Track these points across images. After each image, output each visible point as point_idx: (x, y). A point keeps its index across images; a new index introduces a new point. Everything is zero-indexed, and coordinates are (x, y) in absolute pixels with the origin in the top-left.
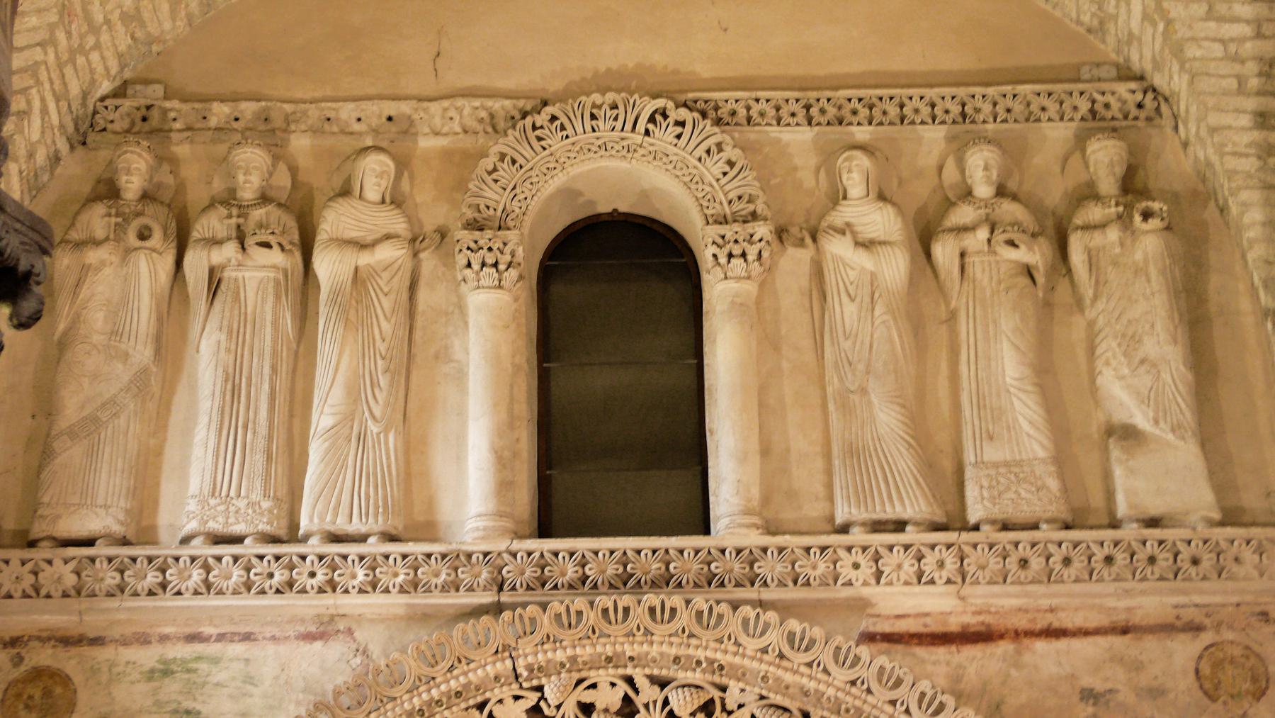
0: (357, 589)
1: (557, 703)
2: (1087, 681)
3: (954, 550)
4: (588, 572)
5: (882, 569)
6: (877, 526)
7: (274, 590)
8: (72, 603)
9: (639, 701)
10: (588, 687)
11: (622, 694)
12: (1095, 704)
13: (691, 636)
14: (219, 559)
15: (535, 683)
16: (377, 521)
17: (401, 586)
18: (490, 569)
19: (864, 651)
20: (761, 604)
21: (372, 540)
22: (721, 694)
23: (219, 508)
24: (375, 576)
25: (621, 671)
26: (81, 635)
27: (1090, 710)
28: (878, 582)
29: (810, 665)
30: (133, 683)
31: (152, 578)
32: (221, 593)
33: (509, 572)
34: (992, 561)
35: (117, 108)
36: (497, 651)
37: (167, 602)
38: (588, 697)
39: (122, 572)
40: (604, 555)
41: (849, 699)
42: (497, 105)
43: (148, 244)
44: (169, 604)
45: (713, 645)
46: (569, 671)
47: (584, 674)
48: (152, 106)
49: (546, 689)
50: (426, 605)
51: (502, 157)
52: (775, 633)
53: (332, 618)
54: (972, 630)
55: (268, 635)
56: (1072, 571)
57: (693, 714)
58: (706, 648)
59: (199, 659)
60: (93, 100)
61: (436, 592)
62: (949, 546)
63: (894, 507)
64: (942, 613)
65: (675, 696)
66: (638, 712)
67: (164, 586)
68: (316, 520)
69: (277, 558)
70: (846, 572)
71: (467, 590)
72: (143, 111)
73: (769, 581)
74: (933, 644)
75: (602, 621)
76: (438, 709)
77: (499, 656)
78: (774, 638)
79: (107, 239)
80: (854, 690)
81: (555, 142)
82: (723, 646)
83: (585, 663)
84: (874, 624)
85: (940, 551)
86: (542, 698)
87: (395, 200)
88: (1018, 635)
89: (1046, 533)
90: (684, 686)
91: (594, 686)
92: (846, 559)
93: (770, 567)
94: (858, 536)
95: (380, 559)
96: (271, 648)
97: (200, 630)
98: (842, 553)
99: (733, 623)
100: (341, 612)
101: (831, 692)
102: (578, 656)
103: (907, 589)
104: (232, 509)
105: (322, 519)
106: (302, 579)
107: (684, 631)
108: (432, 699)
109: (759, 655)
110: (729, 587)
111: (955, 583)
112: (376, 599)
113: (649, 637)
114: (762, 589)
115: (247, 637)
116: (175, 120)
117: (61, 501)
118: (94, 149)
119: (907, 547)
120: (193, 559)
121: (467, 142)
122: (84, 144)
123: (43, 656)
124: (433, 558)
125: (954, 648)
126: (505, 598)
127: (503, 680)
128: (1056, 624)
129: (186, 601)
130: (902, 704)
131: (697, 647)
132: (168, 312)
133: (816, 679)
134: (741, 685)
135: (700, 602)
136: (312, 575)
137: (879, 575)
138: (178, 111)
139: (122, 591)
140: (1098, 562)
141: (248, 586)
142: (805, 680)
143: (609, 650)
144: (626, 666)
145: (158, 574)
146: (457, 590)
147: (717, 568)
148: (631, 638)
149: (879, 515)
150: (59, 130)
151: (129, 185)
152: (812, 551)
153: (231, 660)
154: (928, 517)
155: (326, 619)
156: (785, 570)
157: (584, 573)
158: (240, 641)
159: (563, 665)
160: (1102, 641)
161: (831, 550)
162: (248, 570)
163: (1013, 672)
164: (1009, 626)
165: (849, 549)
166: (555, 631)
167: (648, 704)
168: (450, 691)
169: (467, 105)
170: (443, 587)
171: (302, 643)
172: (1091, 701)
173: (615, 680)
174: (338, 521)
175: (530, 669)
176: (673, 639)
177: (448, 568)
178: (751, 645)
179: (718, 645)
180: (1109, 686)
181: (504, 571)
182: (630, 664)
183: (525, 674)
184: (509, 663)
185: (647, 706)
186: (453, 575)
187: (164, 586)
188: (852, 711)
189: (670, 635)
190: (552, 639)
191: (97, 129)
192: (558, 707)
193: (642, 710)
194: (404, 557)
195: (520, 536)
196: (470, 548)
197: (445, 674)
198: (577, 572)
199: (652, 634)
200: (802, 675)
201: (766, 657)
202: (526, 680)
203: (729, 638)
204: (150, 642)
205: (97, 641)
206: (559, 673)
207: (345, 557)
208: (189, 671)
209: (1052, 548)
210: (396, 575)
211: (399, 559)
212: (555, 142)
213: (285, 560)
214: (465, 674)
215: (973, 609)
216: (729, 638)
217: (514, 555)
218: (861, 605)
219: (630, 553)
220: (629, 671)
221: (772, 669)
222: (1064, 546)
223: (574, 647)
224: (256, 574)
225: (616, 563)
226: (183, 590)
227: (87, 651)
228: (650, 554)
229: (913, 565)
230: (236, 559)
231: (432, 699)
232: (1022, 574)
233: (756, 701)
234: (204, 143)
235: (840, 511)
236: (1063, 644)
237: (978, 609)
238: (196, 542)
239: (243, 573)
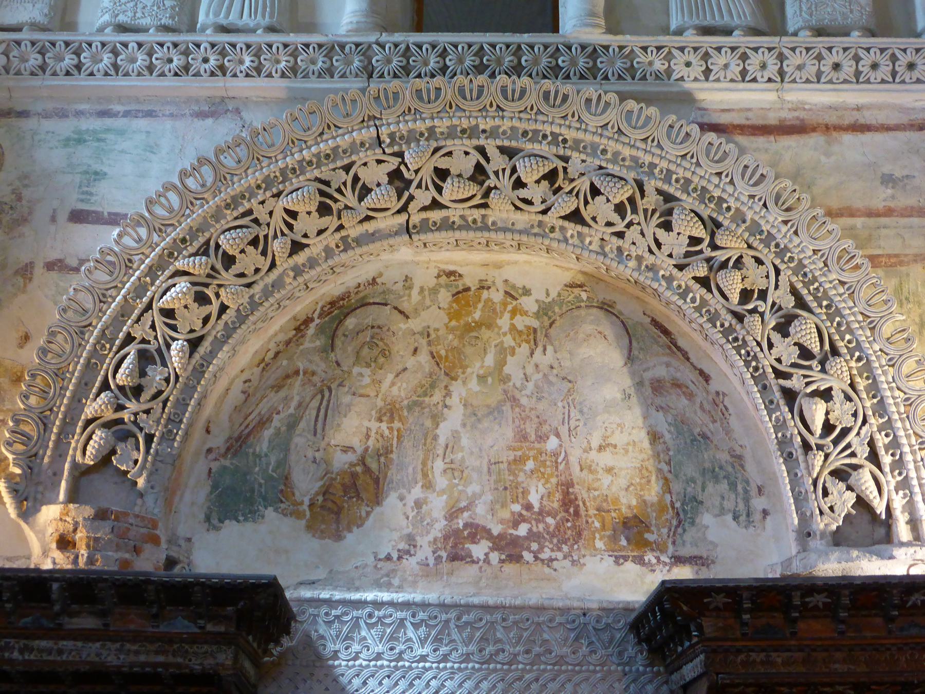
0: (244, 74)
1: (416, 168)
2: (887, 169)
3: (775, 53)
4: (448, 63)
5: (711, 67)
6: (707, 31)
7: (172, 72)
9: (490, 168)
10: (444, 155)
11: (474, 163)
12: (893, 188)
13: (539, 112)
14: (125, 45)
15: (396, 148)
16: (264, 16)
17: (283, 72)
18: (362, 58)
21: (259, 32)
22: (565, 165)
23: (128, 5)
24: (260, 63)
25: (475, 142)
26: (10, 109)
27: (890, 191)
28: (707, 79)
29: (645, 140)
30: (52, 148)
31: (69, 60)
32: (127, 74)
33: (377, 61)
34: (808, 62)
36: (363, 121)
37: (81, 81)
38: (443, 164)
39: (43, 55)
40: (463, 48)
41: (680, 171)
44: (83, 83)
45: (558, 121)
46: (427, 139)
47: (442, 143)
49: (406, 154)
50: (305, 89)
52: (615, 111)
53: (223, 99)
54: (788, 123)
55: (168, 113)
57: (538, 182)
58: (552, 123)
59: (108, 130)
61: (313, 78)
62: (770, 49)
63: (722, 16)
64: (762, 109)
65: (522, 164)
66: (489, 178)
67: (79, 67)
68: (211, 15)
69: (175, 45)
70: (679, 70)
71: (341, 77)
73: (610, 75)
74: (754, 135)
75: (459, 97)
76: (309, 168)
77: (365, 124)
80: (684, 163)
82: (567, 123)
83: (442, 133)
84: (702, 117)
85: (763, 53)
86: (403, 162)
88: (828, 128)
89: (855, 39)
90: (529, 156)
91: (449, 154)
92: (680, 59)
94: (691, 38)
95: (264, 47)
96: (168, 124)
97: (110, 107)
98: (676, 52)
100: (231, 94)
101: (664, 164)
102: (434, 127)
103: (733, 85)
104: (140, 6)
105: (217, 14)
106: (196, 65)
107: (532, 109)
108: (304, 159)
109: (599, 131)
110: (574, 79)
111: (775, 82)
112: (260, 82)
113: (501, 113)
114: (603, 82)
115: (150, 114)
119: (733, 49)
120: (103, 45)
124: (311, 48)
125: (772, 138)
127: (367, 145)
128: (862, 121)
130: (727, 176)
131: (544, 122)
133: (650, 152)
134: (583, 157)
136: (206, 60)
137: (707, 72)
139: (44, 71)
140: (901, 68)
141: (150, 68)
142: (640, 154)
143: (465, 124)
144: (478, 138)
145: (74, 56)
146: (332, 77)
147: (563, 61)
148: (484, 114)
149: (708, 21)
152: (649, 51)
153: (134, 132)
154: (752, 24)
155: (217, 100)
156: (625, 66)
157: (445, 64)
158: (143, 117)
159: (422, 134)
160: (900, 135)
161: (667, 50)
162: (150, 55)
163: (823, 158)
164: (820, 121)
165: (682, 49)
166: (416, 104)
167: (498, 171)
168: (319, 153)
170: (320, 73)
171: (196, 120)
172: (890, 185)
173: (468, 150)
174: (230, 18)
175: (392, 136)
176: (522, 115)
177: (325, 56)
178: (594, 122)
179: (562, 122)
180: (905, 173)
181: (374, 61)
182: (483, 136)
183: (388, 141)
184: (373, 130)
185: (496, 173)
186: (328, 63)
187: (79, 67)
188: (682, 181)
189: (521, 112)
190: (413, 111)
192: (417, 172)
193: (492, 176)
194: (286, 46)
195: (387, 27)
196: (344, 40)
197: (316, 138)
198: (438, 62)
199: (503, 110)
200: (638, 149)
201: (606, 133)
202: (388, 146)
203: (573, 116)
204: (67, 116)
205: (23, 114)
206: (418, 141)
207: (234, 46)
208: (99, 140)
209: (862, 53)
210: (278, 62)
211: (281, 47)
213: (182, 47)
214: (334, 138)
215: (790, 106)
216: (573, 116)
217: (383, 48)
219: (486, 47)
220: (482, 142)
221: (611, 143)
222: (872, 51)
223: (433, 118)
224: (157, 59)
225: (474, 55)
226: (95, 73)
227: (13, 121)
228: (504, 48)
229: (738, 65)
230: (140, 45)
231: (304, 159)
232: (834, 75)
233: (595, 170)
235: (675, 22)
236: (868, 137)
237: (794, 106)
238: (108, 30)
239: (145, 57)
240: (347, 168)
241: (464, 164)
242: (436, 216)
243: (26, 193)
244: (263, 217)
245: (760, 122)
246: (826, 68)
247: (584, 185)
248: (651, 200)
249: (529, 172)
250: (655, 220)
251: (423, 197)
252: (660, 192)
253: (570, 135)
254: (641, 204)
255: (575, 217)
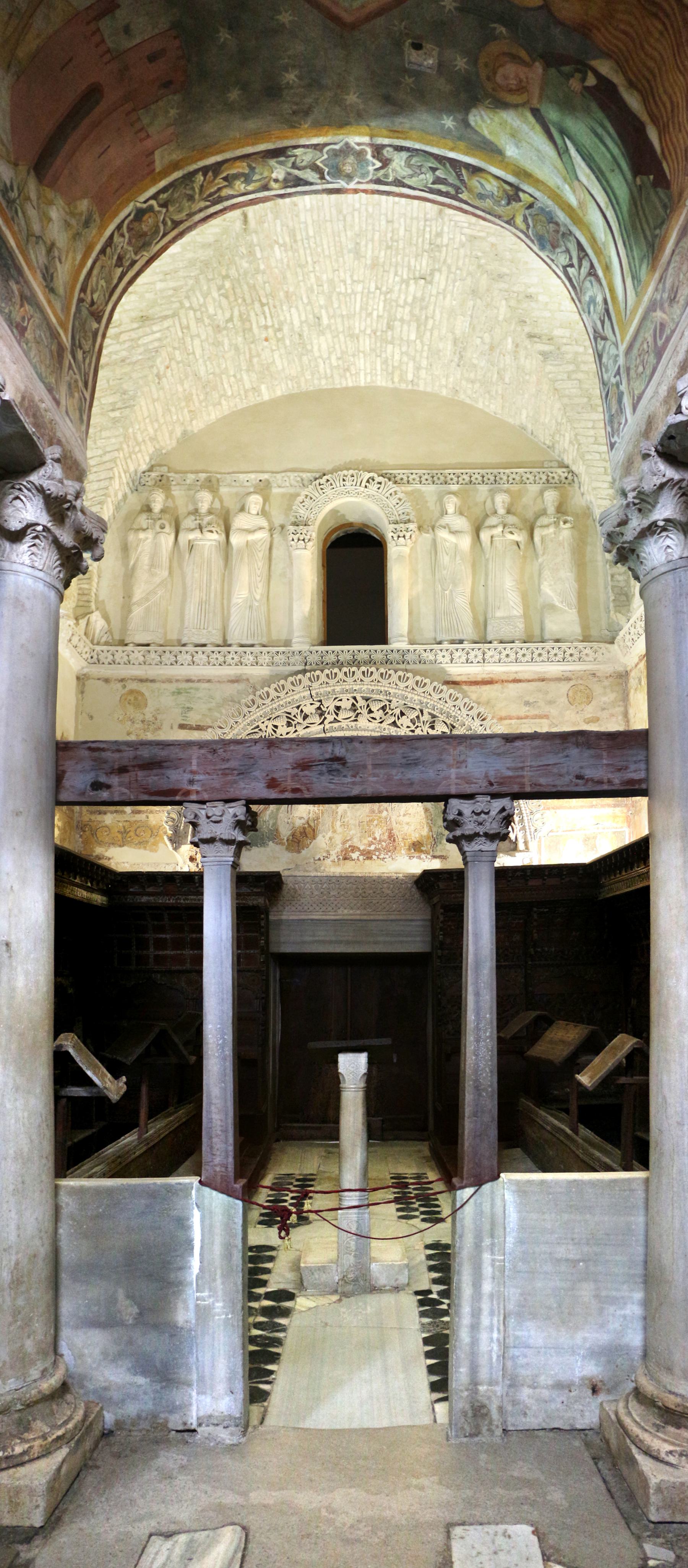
8: (143, 666)
9: (358, 705)
19: (445, 688)
20: (406, 670)
38: (338, 704)
42: (305, 475)
51: (307, 496)
56: (526, 659)
70: (440, 658)
78: (411, 683)
81: (328, 490)
87: (264, 513)
93: (408, 657)
99: (395, 677)
115: (209, 681)
121: (292, 490)
123: (133, 686)
126: (307, 667)
129: (185, 666)
135: (382, 670)
169: (292, 475)
178: (402, 685)
205: (153, 681)
212: (328, 490)
218: (443, 671)
227: (149, 684)
240: (298, 707)
241: (346, 704)
242: (336, 725)
243: (159, 717)
244: (264, 729)
245: (474, 680)
246: (503, 656)
247: (397, 712)
248: (426, 717)
249: (375, 707)
250: (428, 725)
251: (330, 718)
252: (430, 714)
253: (392, 691)
254: (422, 719)
255: (394, 724)
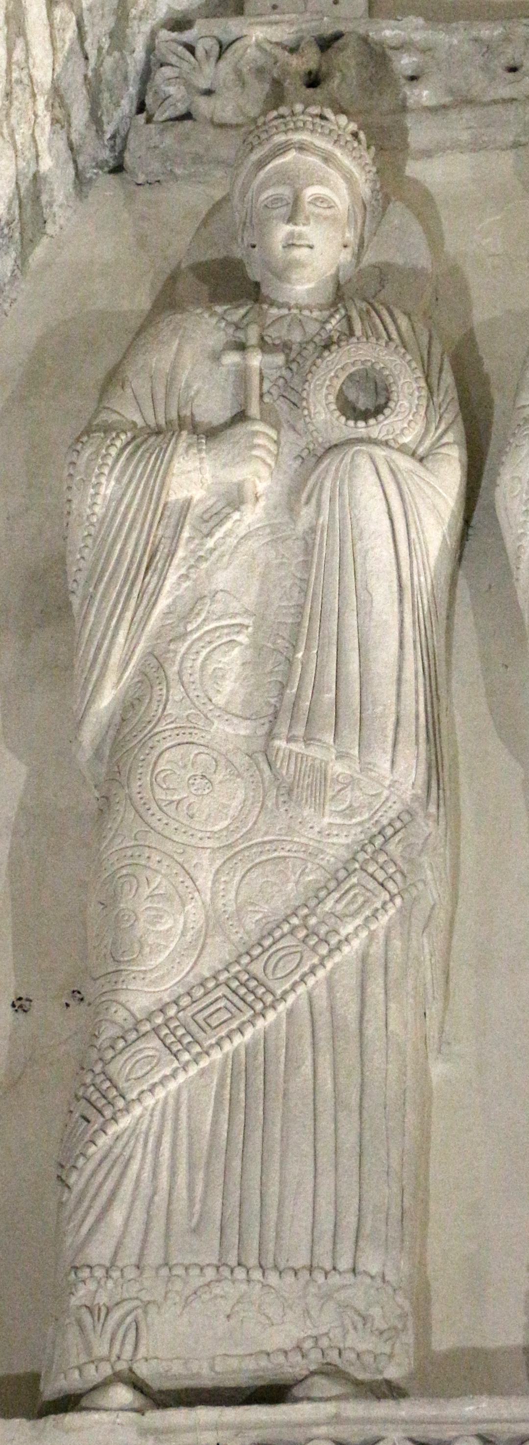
35: (223, 48)
43: (376, 429)
48: (338, 36)
60: (146, 28)
72: (310, 60)
79: (241, 417)
116: (413, 78)
117: (154, 1256)
118: (153, 183)
122: (118, 169)
132: (449, 647)
138: (426, 50)
150: (50, 106)
151: (300, 253)
191: (159, 117)
234: (516, 145)
